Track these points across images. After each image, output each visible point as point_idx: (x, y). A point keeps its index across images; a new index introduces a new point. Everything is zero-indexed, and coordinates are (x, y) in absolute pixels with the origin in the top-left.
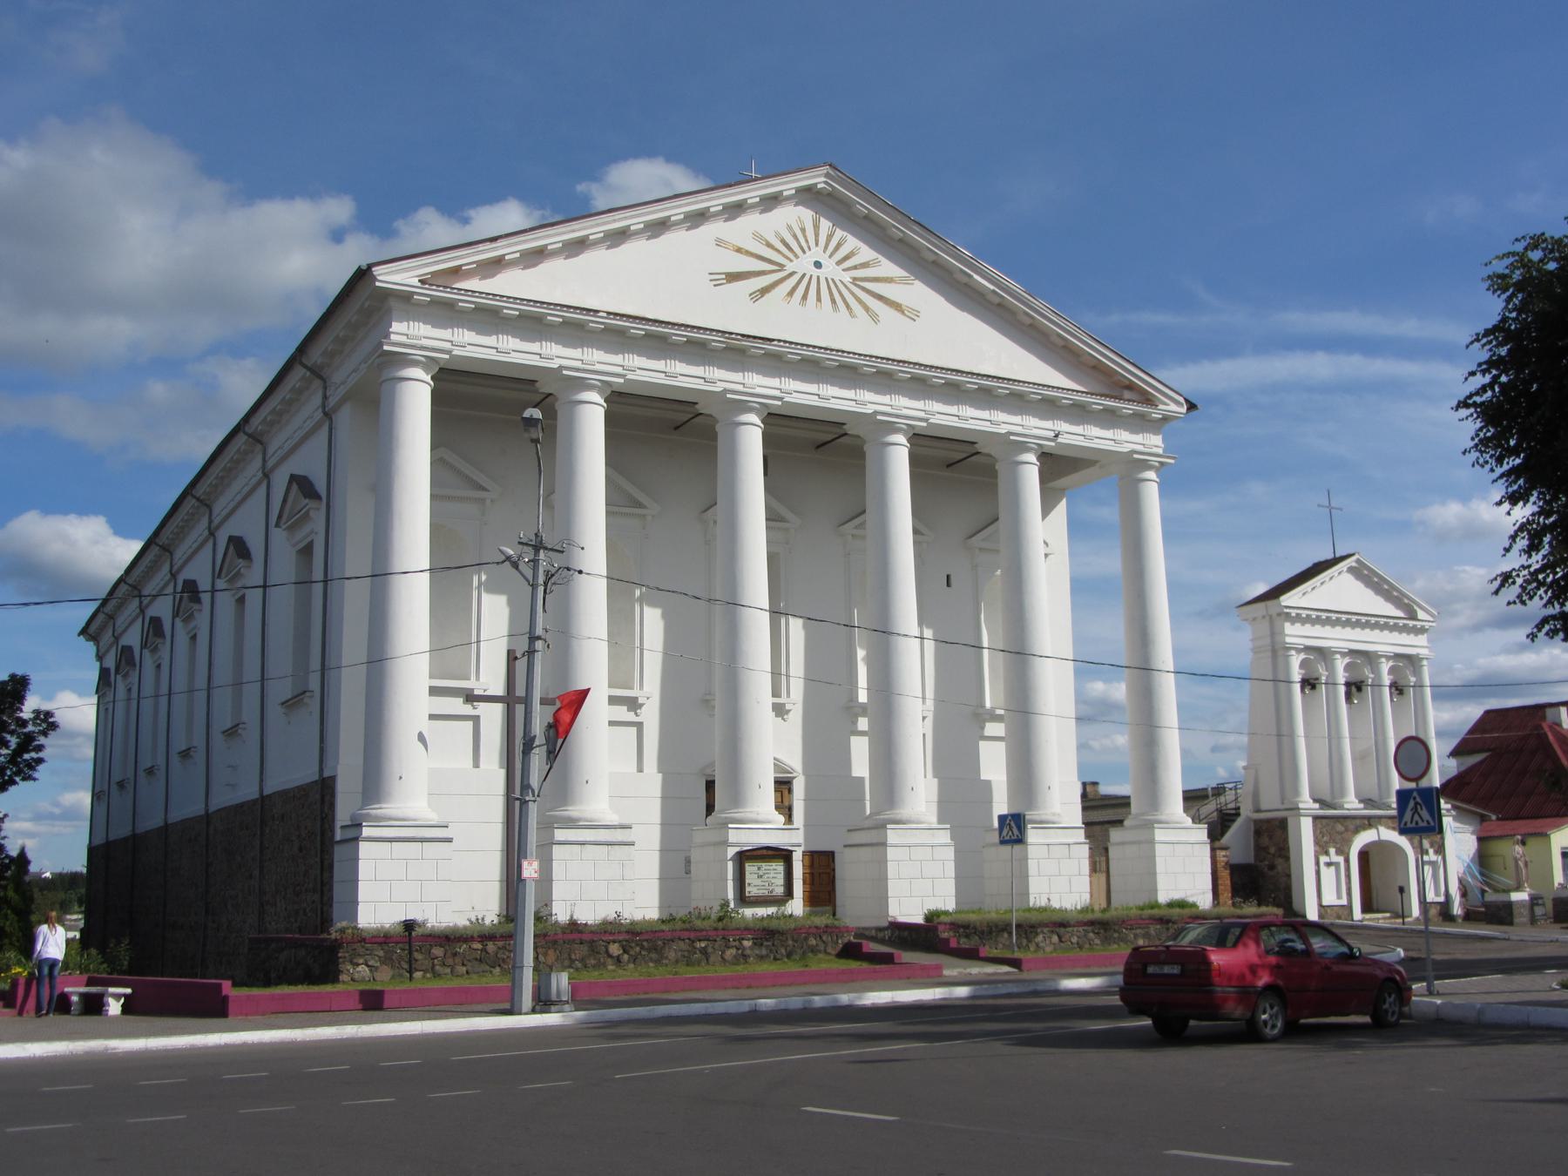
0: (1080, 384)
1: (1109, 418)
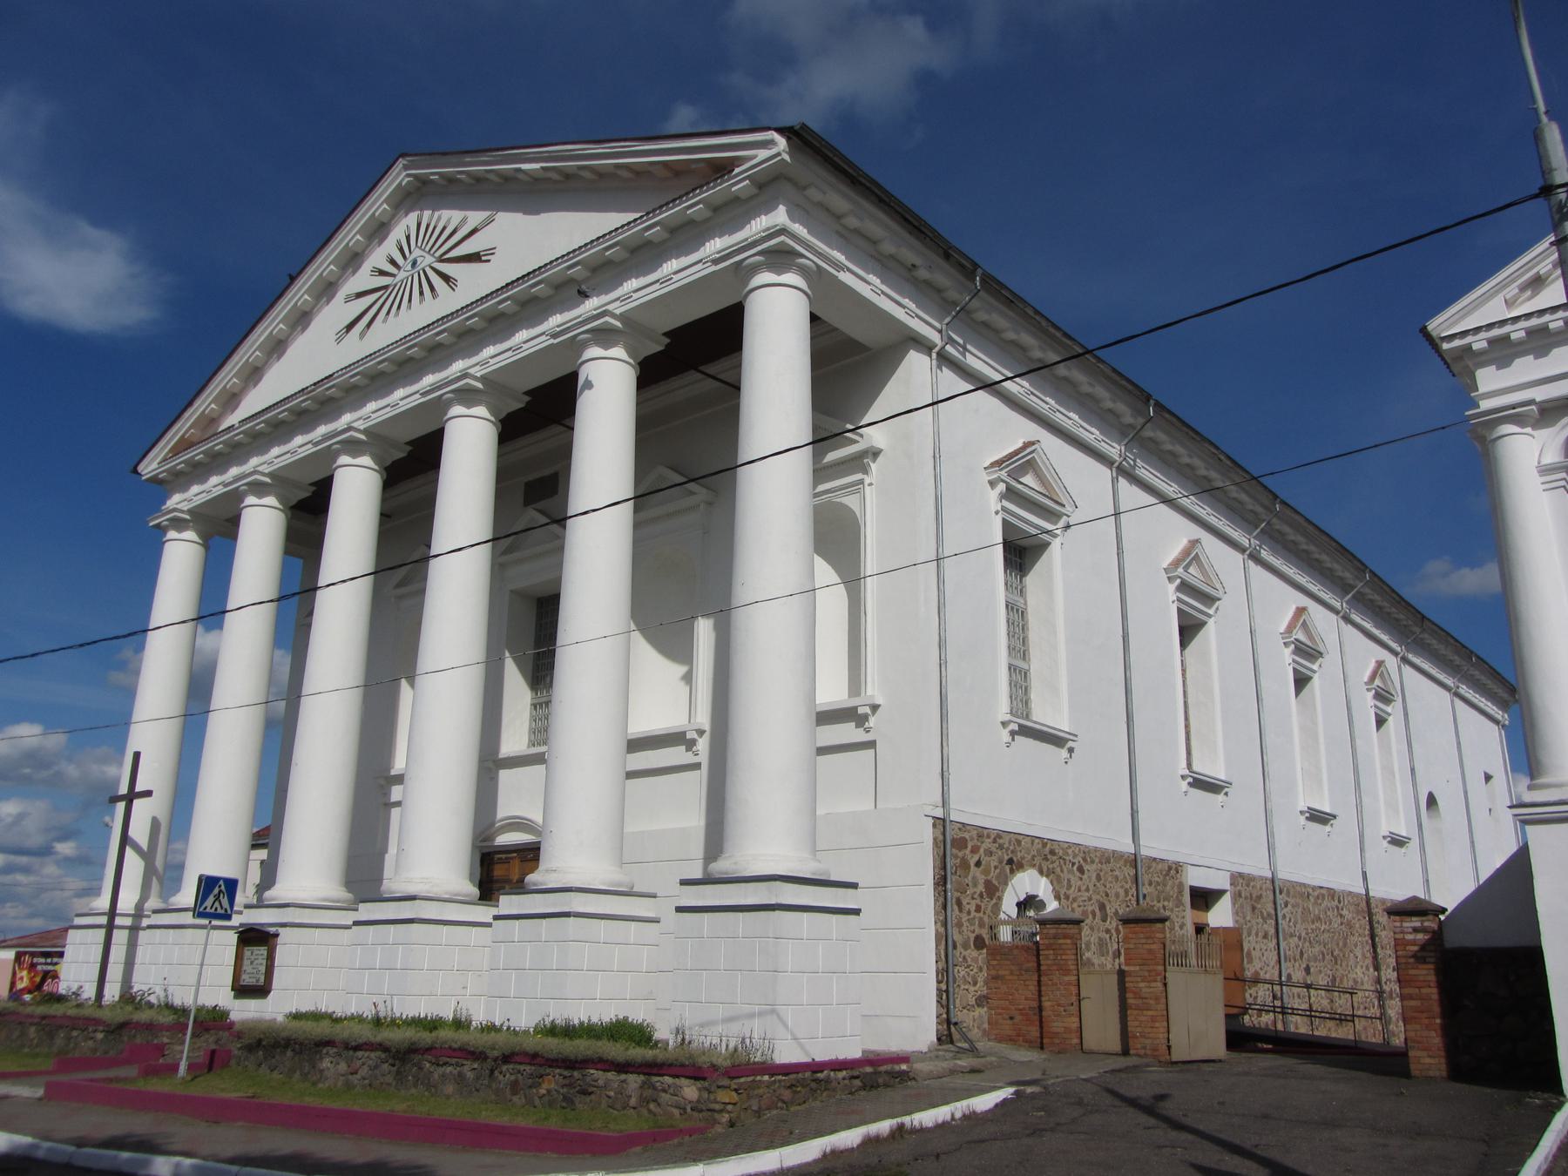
1: (684, 236)
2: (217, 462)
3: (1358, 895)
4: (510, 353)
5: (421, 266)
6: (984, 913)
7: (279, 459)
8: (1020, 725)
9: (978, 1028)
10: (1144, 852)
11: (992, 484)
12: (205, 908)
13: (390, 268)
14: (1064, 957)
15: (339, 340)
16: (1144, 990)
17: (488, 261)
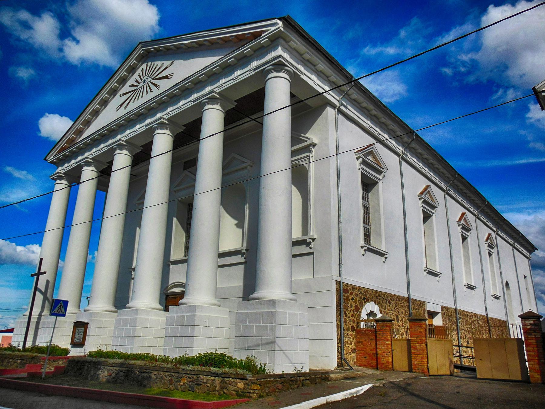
0: (221, 56)
2: (74, 155)
3: (484, 316)
4: (178, 109)
5: (147, 82)
6: (355, 318)
7: (96, 153)
8: (368, 248)
9: (352, 361)
10: (412, 297)
11: (357, 159)
12: (55, 311)
13: (136, 84)
14: (386, 334)
15: (117, 110)
16: (418, 347)
17: (171, 78)
